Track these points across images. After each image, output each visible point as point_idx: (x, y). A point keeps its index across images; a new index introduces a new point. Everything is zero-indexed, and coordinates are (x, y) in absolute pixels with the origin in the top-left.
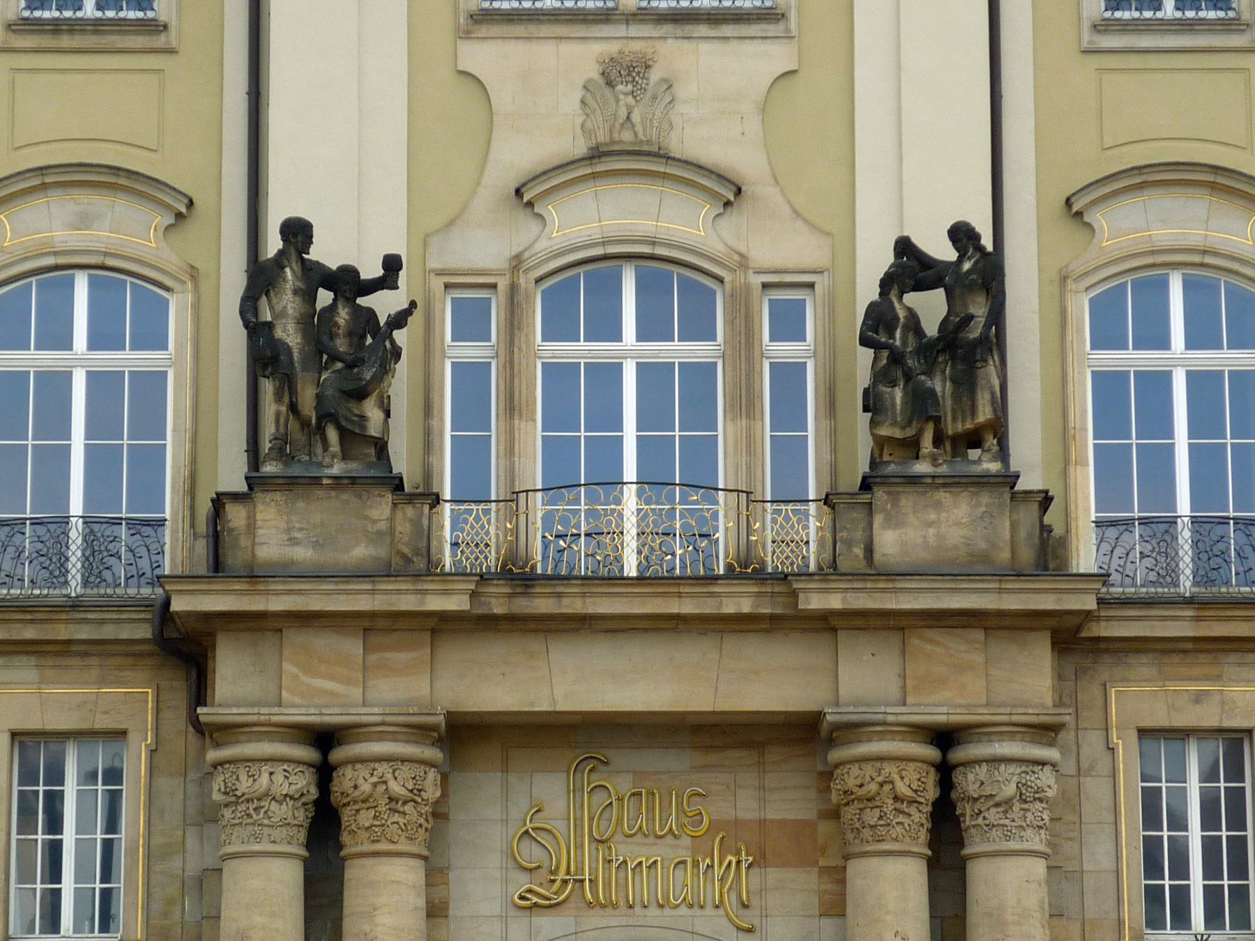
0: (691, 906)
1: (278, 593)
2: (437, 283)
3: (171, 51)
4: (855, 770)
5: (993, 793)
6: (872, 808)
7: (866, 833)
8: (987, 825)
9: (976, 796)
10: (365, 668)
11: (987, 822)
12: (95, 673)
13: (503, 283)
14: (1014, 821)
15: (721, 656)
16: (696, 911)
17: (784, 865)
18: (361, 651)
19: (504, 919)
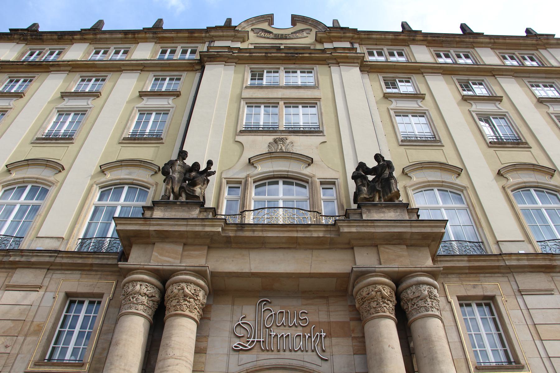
0: (302, 351)
1: (154, 225)
2: (224, 181)
3: (163, 143)
4: (365, 289)
5: (419, 295)
6: (373, 302)
7: (373, 310)
8: (419, 307)
9: (412, 298)
10: (182, 255)
11: (418, 306)
12: (98, 276)
13: (243, 181)
14: (428, 305)
15: (312, 256)
16: (304, 353)
17: (338, 337)
18: (182, 250)
19: (228, 355)
